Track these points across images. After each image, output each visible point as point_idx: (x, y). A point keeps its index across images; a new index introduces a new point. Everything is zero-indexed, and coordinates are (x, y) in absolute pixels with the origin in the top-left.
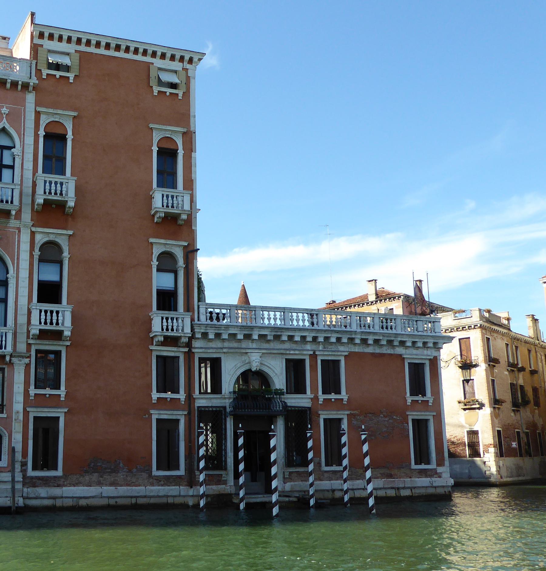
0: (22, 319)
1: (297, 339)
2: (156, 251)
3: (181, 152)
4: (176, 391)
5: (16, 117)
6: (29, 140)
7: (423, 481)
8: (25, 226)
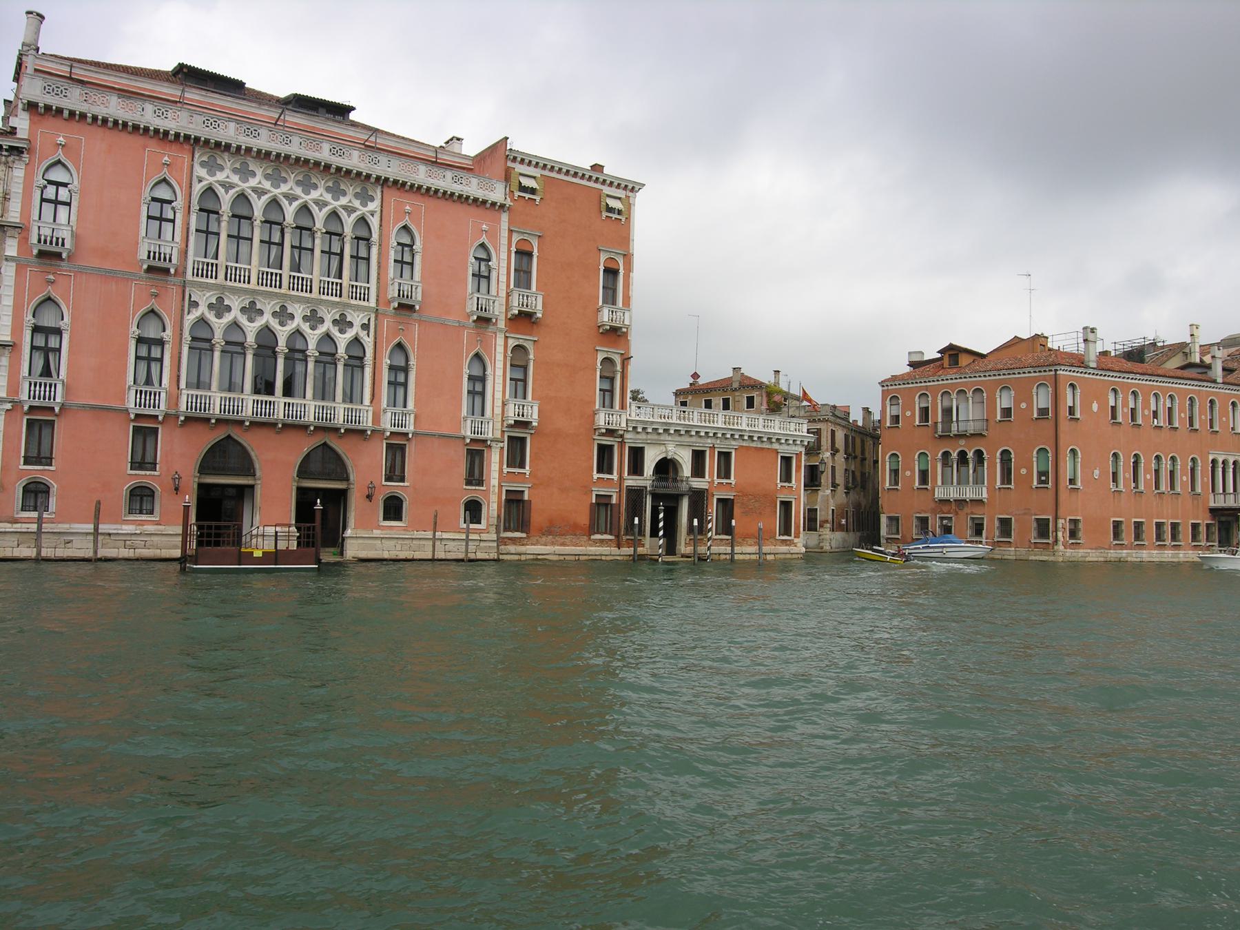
0: (498, 411)
1: (702, 434)
2: (600, 357)
3: (622, 271)
4: (610, 472)
5: (493, 234)
6: (504, 256)
7: (784, 549)
8: (501, 330)
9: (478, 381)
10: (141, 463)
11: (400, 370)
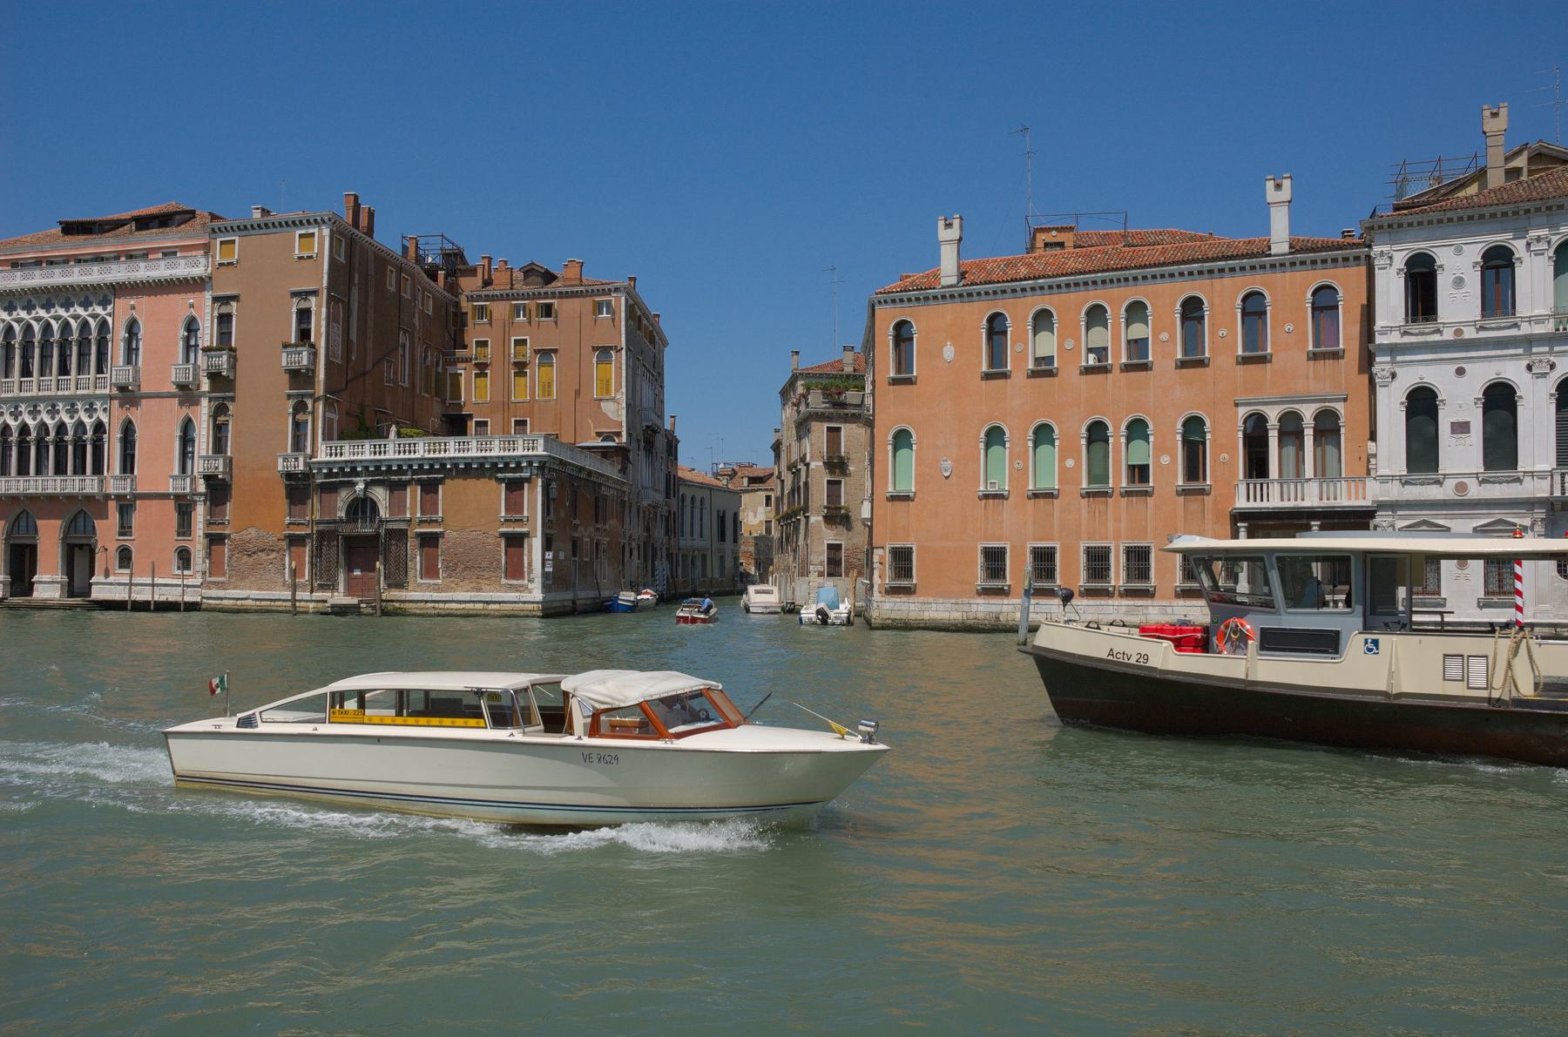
3: (313, 309)
7: (512, 596)
9: (187, 439)
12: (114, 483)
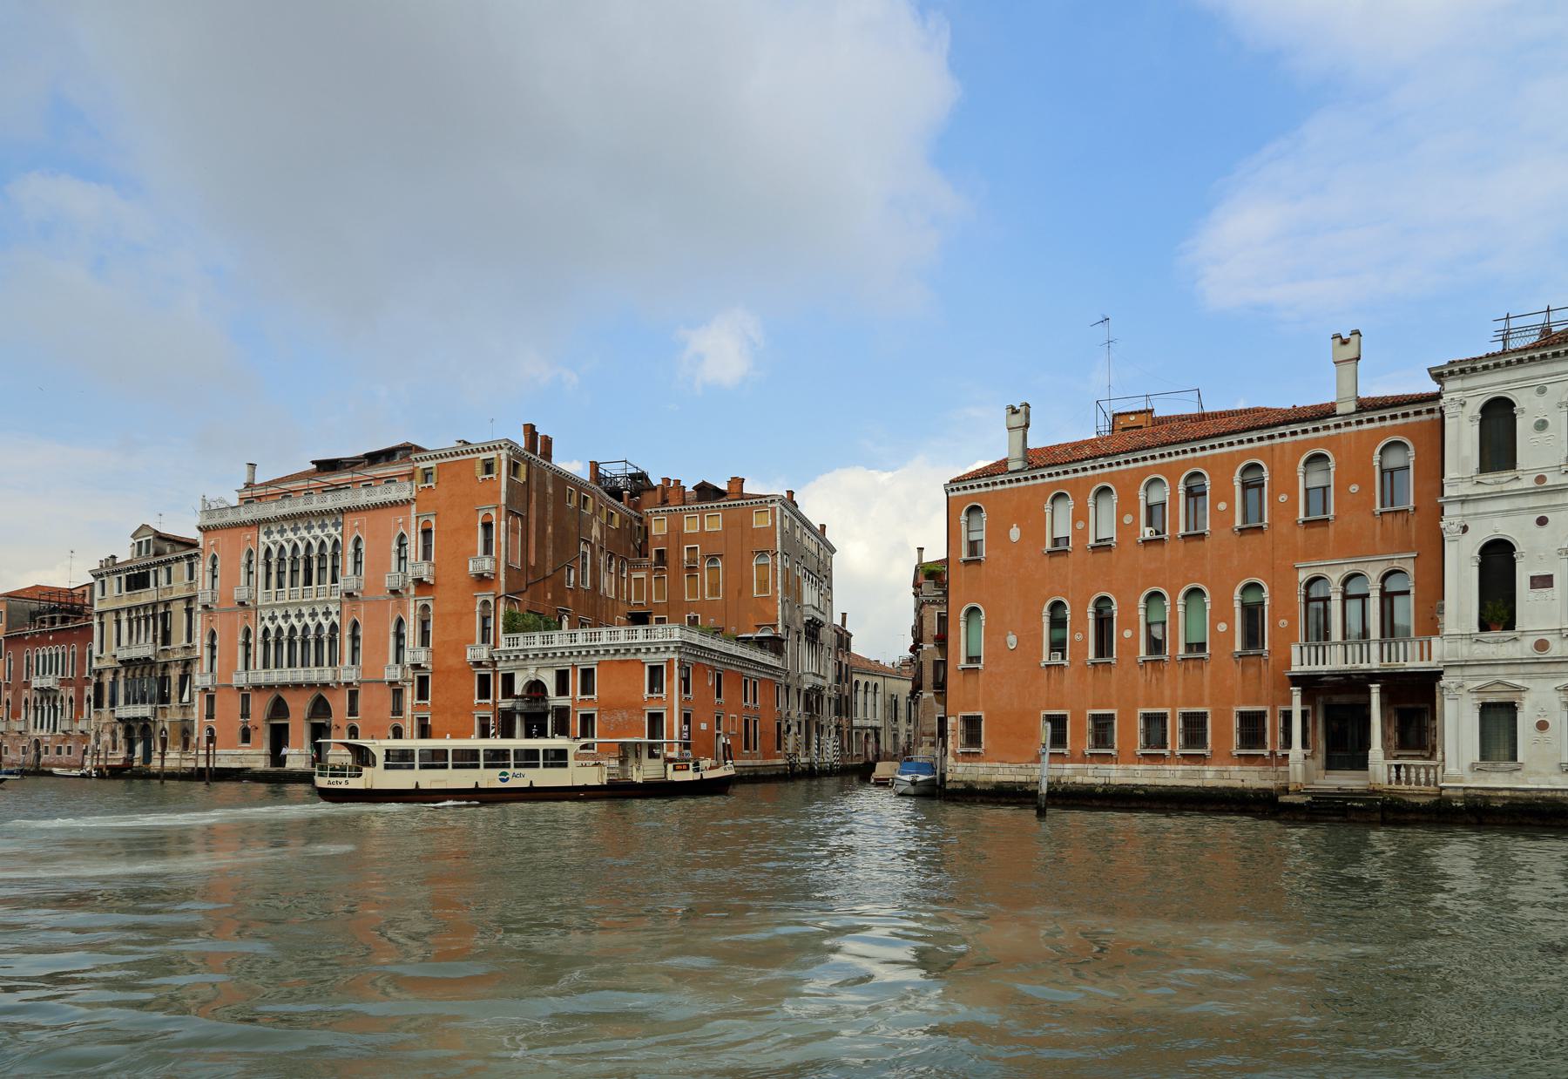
2: (479, 601)
5: (406, 524)
9: (400, 636)
10: (245, 715)
11: (355, 638)
12: (348, 674)
